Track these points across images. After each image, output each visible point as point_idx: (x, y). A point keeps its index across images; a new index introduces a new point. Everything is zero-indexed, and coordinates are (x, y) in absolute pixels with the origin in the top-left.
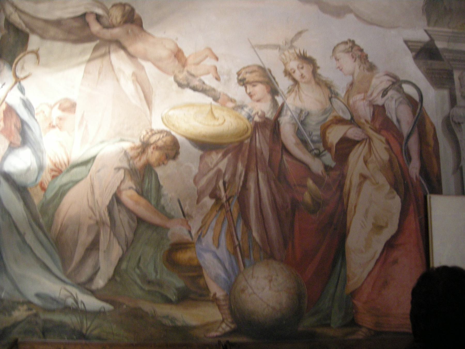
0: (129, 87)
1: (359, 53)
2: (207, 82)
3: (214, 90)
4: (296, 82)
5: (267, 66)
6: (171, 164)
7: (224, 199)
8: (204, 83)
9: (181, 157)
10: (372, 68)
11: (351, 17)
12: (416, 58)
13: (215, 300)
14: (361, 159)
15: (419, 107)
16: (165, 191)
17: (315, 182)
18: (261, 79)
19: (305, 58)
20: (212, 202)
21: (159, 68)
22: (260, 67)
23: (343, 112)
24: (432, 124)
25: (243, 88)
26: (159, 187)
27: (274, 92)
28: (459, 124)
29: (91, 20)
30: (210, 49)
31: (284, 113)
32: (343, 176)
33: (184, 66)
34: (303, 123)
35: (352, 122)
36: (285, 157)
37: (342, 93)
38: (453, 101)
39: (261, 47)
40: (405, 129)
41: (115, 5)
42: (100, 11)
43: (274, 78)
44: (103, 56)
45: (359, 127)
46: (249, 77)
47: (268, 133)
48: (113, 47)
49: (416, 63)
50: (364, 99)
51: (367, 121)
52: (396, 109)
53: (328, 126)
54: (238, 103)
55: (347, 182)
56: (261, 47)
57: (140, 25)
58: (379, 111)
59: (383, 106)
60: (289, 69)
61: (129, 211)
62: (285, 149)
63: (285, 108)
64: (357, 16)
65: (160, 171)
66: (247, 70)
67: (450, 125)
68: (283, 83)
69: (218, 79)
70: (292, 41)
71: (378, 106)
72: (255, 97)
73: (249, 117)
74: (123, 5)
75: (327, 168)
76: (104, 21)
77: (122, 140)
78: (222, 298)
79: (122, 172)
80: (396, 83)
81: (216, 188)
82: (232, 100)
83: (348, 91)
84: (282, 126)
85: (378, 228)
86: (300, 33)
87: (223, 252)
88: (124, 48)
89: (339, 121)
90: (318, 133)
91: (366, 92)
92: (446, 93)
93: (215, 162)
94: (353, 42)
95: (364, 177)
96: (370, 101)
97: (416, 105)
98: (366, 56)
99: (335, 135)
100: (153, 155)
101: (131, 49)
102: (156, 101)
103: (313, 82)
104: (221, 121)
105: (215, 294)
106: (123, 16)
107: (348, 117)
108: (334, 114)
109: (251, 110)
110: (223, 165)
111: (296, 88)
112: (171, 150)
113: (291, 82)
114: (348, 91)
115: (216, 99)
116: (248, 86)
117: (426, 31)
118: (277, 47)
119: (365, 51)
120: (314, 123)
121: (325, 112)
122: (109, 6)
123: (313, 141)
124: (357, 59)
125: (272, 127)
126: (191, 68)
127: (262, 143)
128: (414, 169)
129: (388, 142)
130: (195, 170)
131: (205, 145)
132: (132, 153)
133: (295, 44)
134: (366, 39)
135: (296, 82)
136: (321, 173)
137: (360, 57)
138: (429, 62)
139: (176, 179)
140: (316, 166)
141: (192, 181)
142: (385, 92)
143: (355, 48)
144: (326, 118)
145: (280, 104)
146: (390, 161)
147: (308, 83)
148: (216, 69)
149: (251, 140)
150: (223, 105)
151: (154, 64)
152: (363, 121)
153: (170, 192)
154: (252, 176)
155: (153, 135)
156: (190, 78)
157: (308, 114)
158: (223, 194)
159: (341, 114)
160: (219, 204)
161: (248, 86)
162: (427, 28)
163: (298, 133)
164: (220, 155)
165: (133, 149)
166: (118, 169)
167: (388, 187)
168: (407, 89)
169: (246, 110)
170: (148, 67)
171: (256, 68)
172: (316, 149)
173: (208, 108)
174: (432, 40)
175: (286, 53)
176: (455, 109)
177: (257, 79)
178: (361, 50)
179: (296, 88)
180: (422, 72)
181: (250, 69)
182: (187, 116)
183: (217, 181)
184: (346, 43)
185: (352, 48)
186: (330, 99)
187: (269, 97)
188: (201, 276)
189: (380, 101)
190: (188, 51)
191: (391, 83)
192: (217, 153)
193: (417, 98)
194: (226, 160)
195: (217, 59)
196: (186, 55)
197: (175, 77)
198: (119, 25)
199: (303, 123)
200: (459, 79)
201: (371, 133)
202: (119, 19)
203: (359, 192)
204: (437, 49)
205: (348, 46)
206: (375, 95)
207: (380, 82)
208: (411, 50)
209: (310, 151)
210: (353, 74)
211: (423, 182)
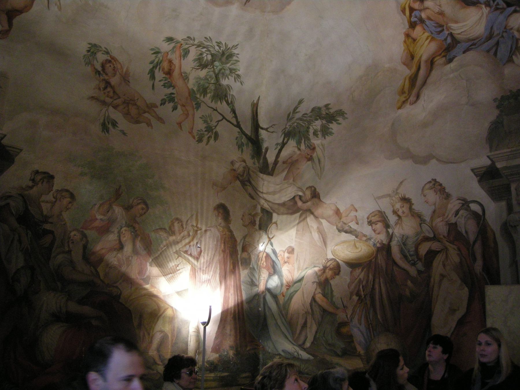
0: (316, 236)
1: (439, 187)
2: (352, 226)
3: (356, 230)
4: (399, 216)
5: (383, 210)
6: (337, 277)
7: (363, 296)
8: (351, 227)
9: (342, 273)
10: (448, 196)
11: (434, 161)
12: (480, 181)
13: (359, 355)
14: (441, 263)
15: (482, 219)
16: (335, 294)
17: (412, 282)
18: (380, 219)
19: (406, 200)
20: (357, 298)
21: (329, 222)
22: (379, 211)
23: (429, 233)
24: (492, 231)
25: (370, 227)
26: (332, 291)
27: (387, 226)
28: (515, 226)
29: (297, 199)
30: (353, 205)
31: (393, 239)
32: (429, 277)
33: (340, 219)
34: (404, 244)
35: (435, 238)
36: (395, 268)
37: (428, 219)
38: (510, 209)
39: (380, 198)
40: (472, 237)
41: (307, 188)
42: (300, 194)
43: (387, 217)
44: (304, 219)
45: (439, 242)
46: (374, 219)
47: (384, 253)
48: (308, 213)
49: (480, 185)
50: (442, 221)
51: (444, 236)
52: (465, 223)
53: (419, 244)
54: (368, 237)
55: (432, 280)
56: (380, 198)
57: (319, 198)
58: (453, 227)
59: (456, 224)
60: (395, 209)
61: (320, 306)
62: (395, 263)
63: (394, 235)
64: (438, 160)
65: (332, 282)
66: (373, 215)
67: (507, 229)
68: (392, 219)
69: (357, 224)
70: (397, 189)
71: (452, 224)
72: (377, 232)
73: (374, 245)
74: (311, 187)
75: (419, 272)
76: (303, 199)
77: (315, 267)
78: (363, 354)
79: (315, 284)
80: (465, 203)
81: (359, 291)
82: (365, 236)
83: (432, 217)
84: (392, 248)
85: (452, 311)
86: (401, 183)
87: (363, 328)
88: (312, 213)
89: (426, 239)
90: (414, 249)
91: (444, 215)
92: (503, 204)
93: (358, 274)
94: (435, 180)
95: (442, 276)
96: (447, 221)
97: (479, 218)
98: (444, 188)
99: (423, 249)
100: (329, 273)
101: (316, 213)
102: (328, 242)
103: (410, 215)
104: (360, 249)
105: (359, 352)
106: (311, 194)
107: (432, 235)
108: (422, 235)
109: (375, 240)
110: (361, 276)
111: (400, 222)
112: (337, 269)
113: (397, 218)
114: (432, 217)
115: (357, 237)
116: (373, 225)
117: (488, 157)
118: (389, 195)
119: (443, 185)
120: (411, 243)
121: (417, 234)
122: (304, 190)
123: (411, 256)
124: (438, 192)
125: (385, 249)
126: (344, 219)
127: (381, 260)
128: (478, 266)
129: (459, 250)
130: (348, 280)
131: (353, 265)
132: (319, 273)
133: (399, 191)
134: (445, 175)
135: (399, 216)
136: (415, 276)
137: (440, 191)
138: (491, 181)
139: (341, 285)
140: (413, 271)
141: (347, 286)
142: (457, 213)
143: (437, 184)
144: (418, 238)
145: (391, 234)
146: (461, 262)
147: (406, 216)
148: (356, 216)
149: (376, 259)
150: (361, 240)
151: (327, 221)
152: (442, 237)
153: (337, 294)
154: (377, 280)
155: (328, 261)
156: (344, 225)
157: (407, 237)
158: (362, 293)
159: (427, 235)
160: (361, 300)
161: (373, 225)
162: (489, 154)
163: (402, 251)
164: (360, 270)
165: (319, 271)
166: (314, 282)
167: (459, 282)
168: (474, 207)
169: (372, 240)
170: (324, 221)
171: (377, 213)
172: (412, 260)
173: (353, 242)
174: (493, 163)
175: (394, 198)
176: (511, 215)
177: (378, 219)
178: (441, 185)
179: (400, 222)
180: (485, 191)
181: (373, 214)
182: (343, 248)
183: (359, 286)
184: (430, 182)
185: (434, 184)
186: (420, 224)
187: (385, 230)
188: (353, 342)
189: (453, 220)
190: (342, 209)
191: (461, 205)
192: (359, 269)
193: (480, 212)
194: (363, 273)
195: (356, 211)
196: (341, 211)
197: (337, 226)
198: (310, 200)
199: (404, 244)
200: (516, 190)
201: (447, 244)
202: (310, 196)
203: (439, 287)
204: (497, 169)
205: (431, 184)
206: (450, 216)
207: (454, 205)
208: (476, 176)
209: (409, 262)
210: (435, 204)
211: (485, 275)
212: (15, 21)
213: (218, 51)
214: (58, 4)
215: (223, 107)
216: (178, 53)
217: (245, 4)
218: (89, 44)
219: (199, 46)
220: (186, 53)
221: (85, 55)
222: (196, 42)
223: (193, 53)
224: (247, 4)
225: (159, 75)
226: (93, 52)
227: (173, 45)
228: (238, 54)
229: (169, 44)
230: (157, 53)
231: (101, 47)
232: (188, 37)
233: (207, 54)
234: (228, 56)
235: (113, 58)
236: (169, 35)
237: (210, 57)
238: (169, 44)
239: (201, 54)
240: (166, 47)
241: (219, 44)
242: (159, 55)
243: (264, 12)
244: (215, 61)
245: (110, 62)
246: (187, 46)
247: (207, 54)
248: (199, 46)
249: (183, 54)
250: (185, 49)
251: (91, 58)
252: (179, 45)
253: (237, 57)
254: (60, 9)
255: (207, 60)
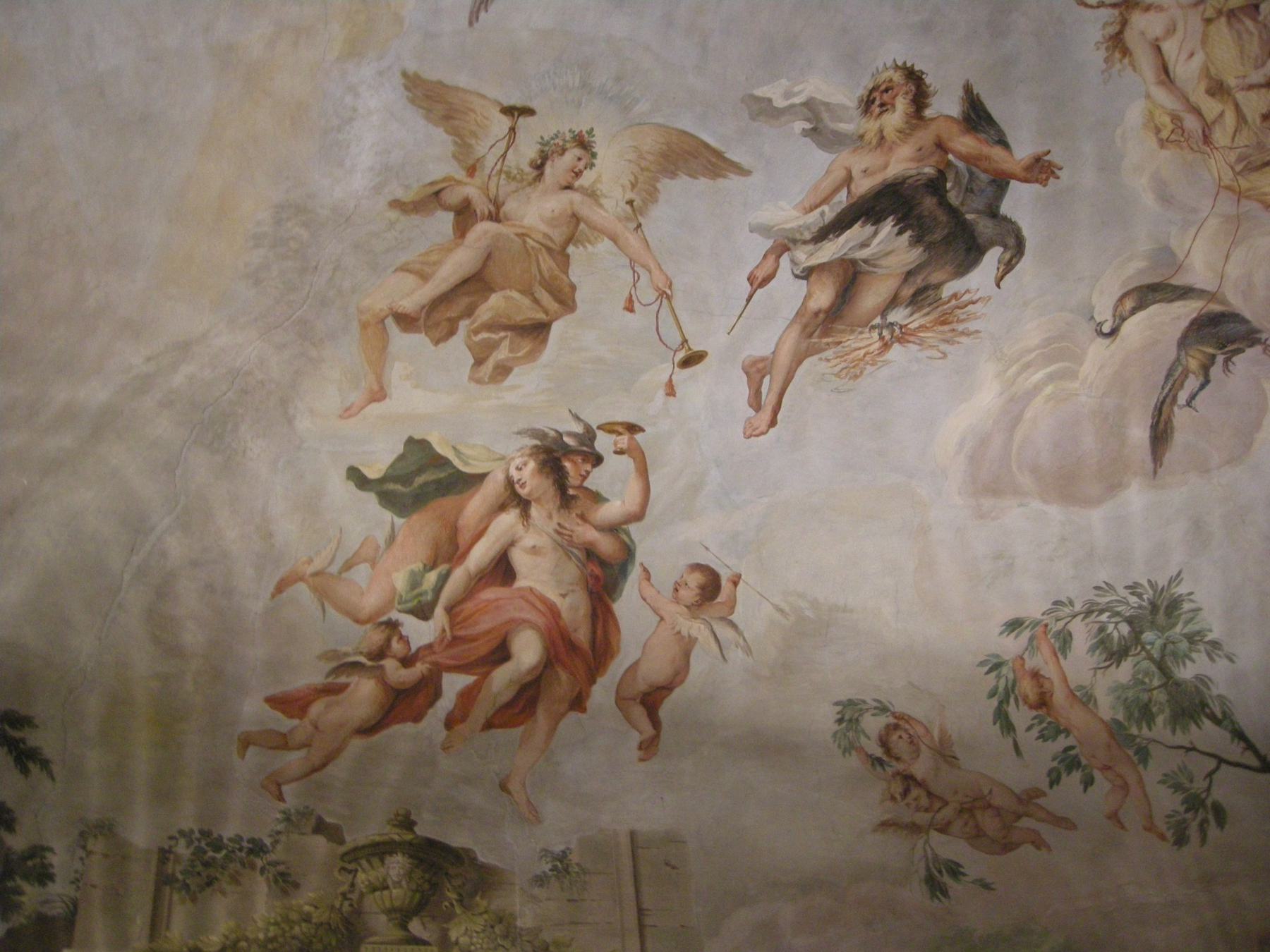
212: (664, 712)
213: (1140, 607)
214: (741, 641)
215: (1207, 734)
216: (1045, 650)
217: (1155, 472)
218: (837, 704)
219: (1088, 613)
220: (1065, 639)
221: (835, 734)
222: (1078, 607)
223: (1082, 634)
224: (1160, 470)
225: (1021, 716)
226: (850, 720)
227: (1026, 634)
228: (1191, 593)
229: (1016, 637)
230: (997, 666)
231: (864, 702)
232: (1056, 603)
233: (1117, 623)
234: (1167, 607)
235: (900, 717)
236: (1011, 615)
237: (1125, 629)
238: (1016, 637)
239: (1102, 629)
240: (1011, 646)
241: (1133, 588)
242: (1004, 670)
243: (1207, 471)
244: (1142, 632)
245: (896, 727)
246: (1060, 624)
247: (1117, 623)
248: (1088, 613)
249: (1057, 645)
250: (1059, 633)
251: (851, 734)
252: (1039, 629)
253: (1192, 601)
254: (748, 651)
255: (1121, 637)
